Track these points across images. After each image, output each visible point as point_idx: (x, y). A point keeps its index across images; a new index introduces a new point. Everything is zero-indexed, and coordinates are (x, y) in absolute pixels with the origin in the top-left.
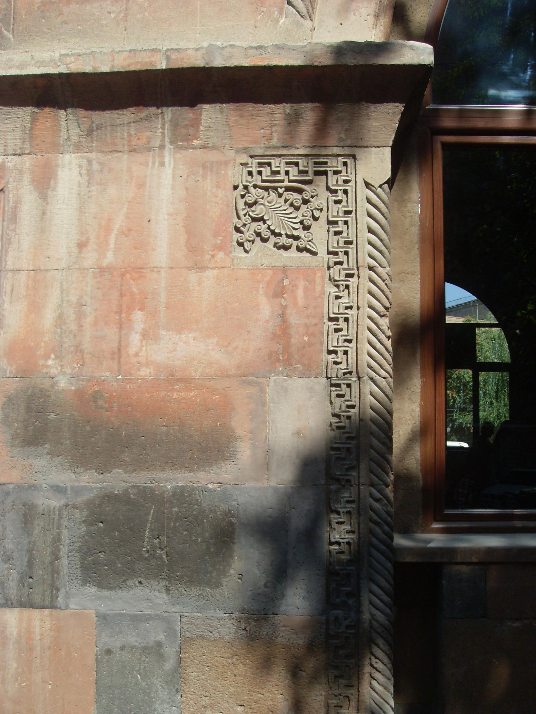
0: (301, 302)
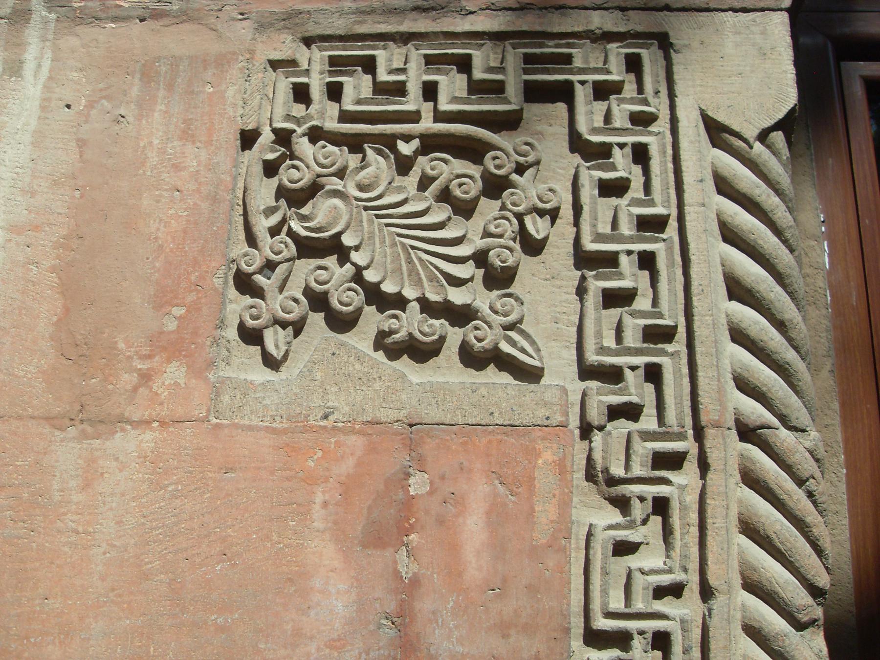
0: (475, 564)
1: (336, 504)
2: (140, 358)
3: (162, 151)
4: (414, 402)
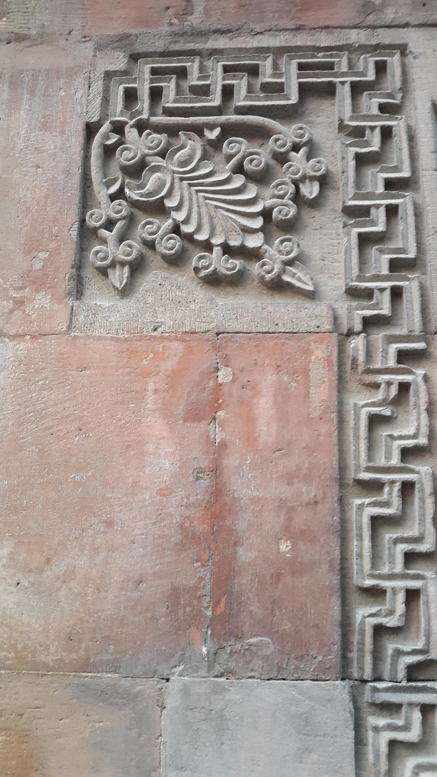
0: (267, 430)
1: (164, 391)
2: (14, 289)
3: (27, 139)
4: (220, 317)
